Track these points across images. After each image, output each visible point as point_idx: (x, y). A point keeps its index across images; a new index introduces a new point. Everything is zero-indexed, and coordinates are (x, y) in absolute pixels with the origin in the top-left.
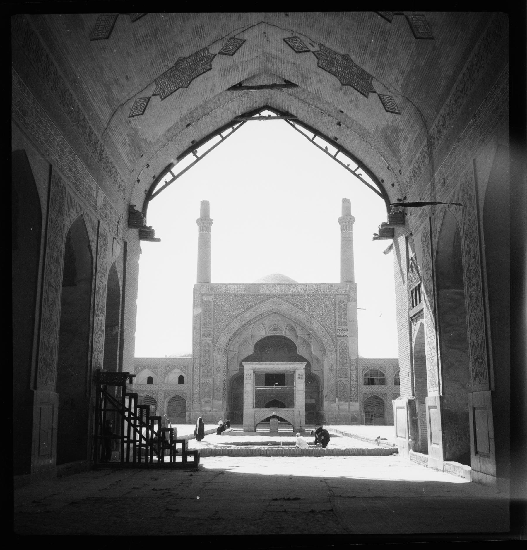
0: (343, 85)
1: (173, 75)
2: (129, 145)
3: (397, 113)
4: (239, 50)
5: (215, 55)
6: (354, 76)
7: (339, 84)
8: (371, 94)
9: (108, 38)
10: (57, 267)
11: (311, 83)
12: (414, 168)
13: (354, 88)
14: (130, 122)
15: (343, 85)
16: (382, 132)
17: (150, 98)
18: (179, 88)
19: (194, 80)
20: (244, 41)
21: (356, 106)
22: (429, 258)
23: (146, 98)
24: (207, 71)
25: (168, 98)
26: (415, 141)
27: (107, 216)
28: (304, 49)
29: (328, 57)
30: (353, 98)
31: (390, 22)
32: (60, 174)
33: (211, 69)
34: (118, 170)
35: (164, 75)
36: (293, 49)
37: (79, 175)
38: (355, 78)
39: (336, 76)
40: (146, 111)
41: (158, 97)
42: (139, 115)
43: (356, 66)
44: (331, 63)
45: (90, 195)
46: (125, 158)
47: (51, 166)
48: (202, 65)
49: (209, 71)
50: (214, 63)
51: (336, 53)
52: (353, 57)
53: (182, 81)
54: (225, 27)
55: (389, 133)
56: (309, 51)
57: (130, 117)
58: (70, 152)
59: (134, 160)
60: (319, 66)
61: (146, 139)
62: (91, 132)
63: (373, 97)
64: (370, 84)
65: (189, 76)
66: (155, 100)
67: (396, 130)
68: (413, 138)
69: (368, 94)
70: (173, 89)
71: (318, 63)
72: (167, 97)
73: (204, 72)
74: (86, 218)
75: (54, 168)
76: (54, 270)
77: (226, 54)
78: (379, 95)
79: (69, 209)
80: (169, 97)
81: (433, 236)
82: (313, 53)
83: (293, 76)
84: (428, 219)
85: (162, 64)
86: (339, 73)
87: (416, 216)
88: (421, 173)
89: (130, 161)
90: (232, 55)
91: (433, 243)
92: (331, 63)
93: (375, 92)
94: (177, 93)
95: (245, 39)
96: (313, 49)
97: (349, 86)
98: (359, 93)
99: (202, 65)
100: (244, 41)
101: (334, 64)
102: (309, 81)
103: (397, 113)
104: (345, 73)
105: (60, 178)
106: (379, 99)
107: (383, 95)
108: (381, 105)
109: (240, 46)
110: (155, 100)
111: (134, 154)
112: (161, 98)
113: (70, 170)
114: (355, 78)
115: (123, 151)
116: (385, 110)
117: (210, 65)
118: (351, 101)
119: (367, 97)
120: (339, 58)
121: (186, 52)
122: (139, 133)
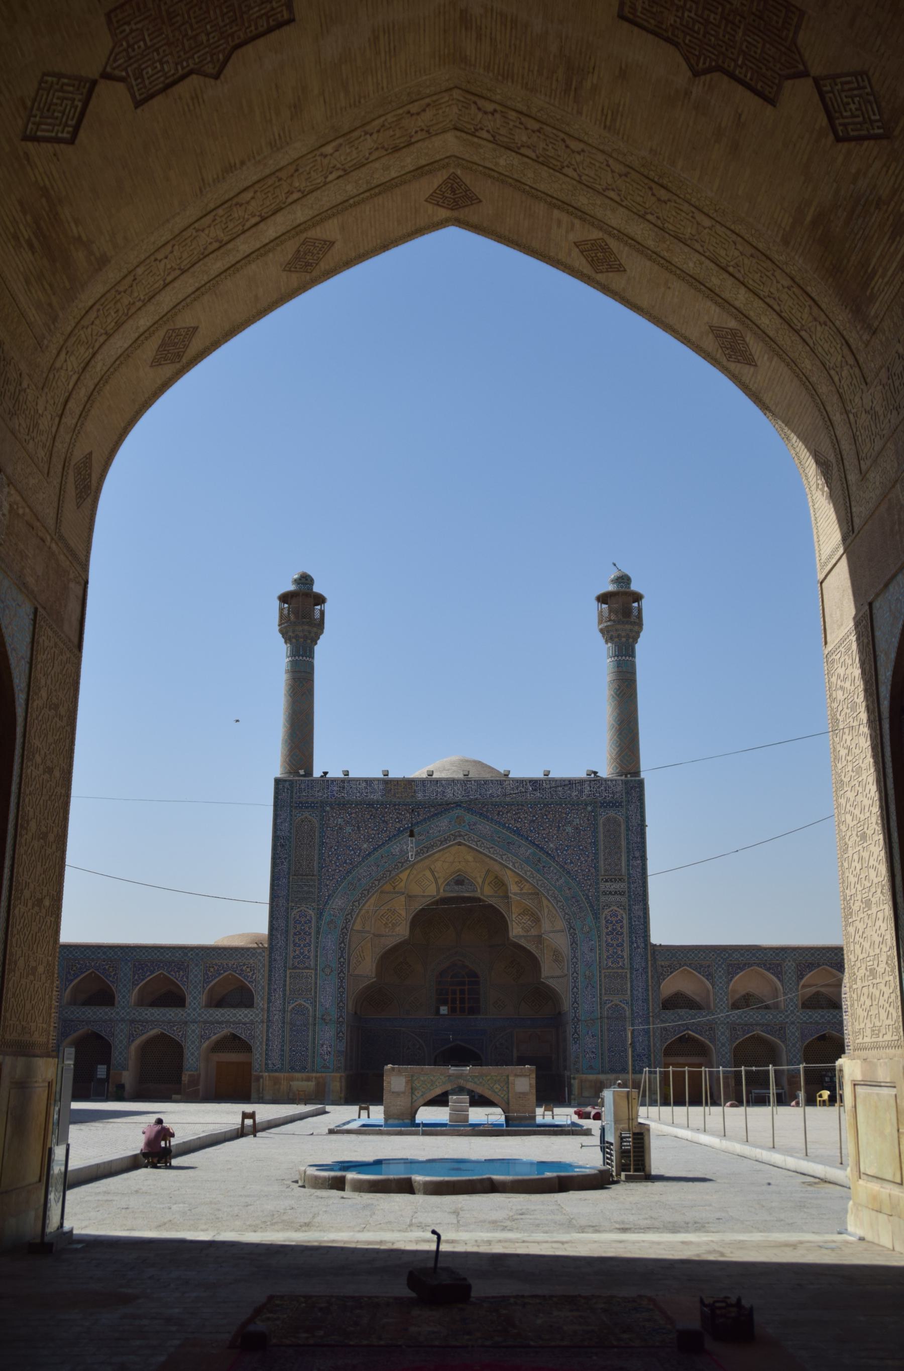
0: (696, 74)
2: (31, 246)
8: (788, 84)
13: (732, 76)
15: (696, 74)
18: (191, 72)
24: (280, 25)
25: (154, 102)
33: (291, 21)
39: (676, 45)
40: (82, 134)
41: (121, 86)
49: (287, 28)
57: (26, 138)
59: (50, 305)
60: (621, 17)
63: (798, 97)
66: (112, 99)
72: (152, 96)
73: (270, 30)
78: (816, 81)
80: (159, 98)
93: (805, 74)
98: (749, 94)
103: (876, 137)
106: (817, 95)
108: (823, 120)
110: (112, 99)
111: (51, 285)
112: (133, 96)
116: (831, 137)
119: (771, 101)
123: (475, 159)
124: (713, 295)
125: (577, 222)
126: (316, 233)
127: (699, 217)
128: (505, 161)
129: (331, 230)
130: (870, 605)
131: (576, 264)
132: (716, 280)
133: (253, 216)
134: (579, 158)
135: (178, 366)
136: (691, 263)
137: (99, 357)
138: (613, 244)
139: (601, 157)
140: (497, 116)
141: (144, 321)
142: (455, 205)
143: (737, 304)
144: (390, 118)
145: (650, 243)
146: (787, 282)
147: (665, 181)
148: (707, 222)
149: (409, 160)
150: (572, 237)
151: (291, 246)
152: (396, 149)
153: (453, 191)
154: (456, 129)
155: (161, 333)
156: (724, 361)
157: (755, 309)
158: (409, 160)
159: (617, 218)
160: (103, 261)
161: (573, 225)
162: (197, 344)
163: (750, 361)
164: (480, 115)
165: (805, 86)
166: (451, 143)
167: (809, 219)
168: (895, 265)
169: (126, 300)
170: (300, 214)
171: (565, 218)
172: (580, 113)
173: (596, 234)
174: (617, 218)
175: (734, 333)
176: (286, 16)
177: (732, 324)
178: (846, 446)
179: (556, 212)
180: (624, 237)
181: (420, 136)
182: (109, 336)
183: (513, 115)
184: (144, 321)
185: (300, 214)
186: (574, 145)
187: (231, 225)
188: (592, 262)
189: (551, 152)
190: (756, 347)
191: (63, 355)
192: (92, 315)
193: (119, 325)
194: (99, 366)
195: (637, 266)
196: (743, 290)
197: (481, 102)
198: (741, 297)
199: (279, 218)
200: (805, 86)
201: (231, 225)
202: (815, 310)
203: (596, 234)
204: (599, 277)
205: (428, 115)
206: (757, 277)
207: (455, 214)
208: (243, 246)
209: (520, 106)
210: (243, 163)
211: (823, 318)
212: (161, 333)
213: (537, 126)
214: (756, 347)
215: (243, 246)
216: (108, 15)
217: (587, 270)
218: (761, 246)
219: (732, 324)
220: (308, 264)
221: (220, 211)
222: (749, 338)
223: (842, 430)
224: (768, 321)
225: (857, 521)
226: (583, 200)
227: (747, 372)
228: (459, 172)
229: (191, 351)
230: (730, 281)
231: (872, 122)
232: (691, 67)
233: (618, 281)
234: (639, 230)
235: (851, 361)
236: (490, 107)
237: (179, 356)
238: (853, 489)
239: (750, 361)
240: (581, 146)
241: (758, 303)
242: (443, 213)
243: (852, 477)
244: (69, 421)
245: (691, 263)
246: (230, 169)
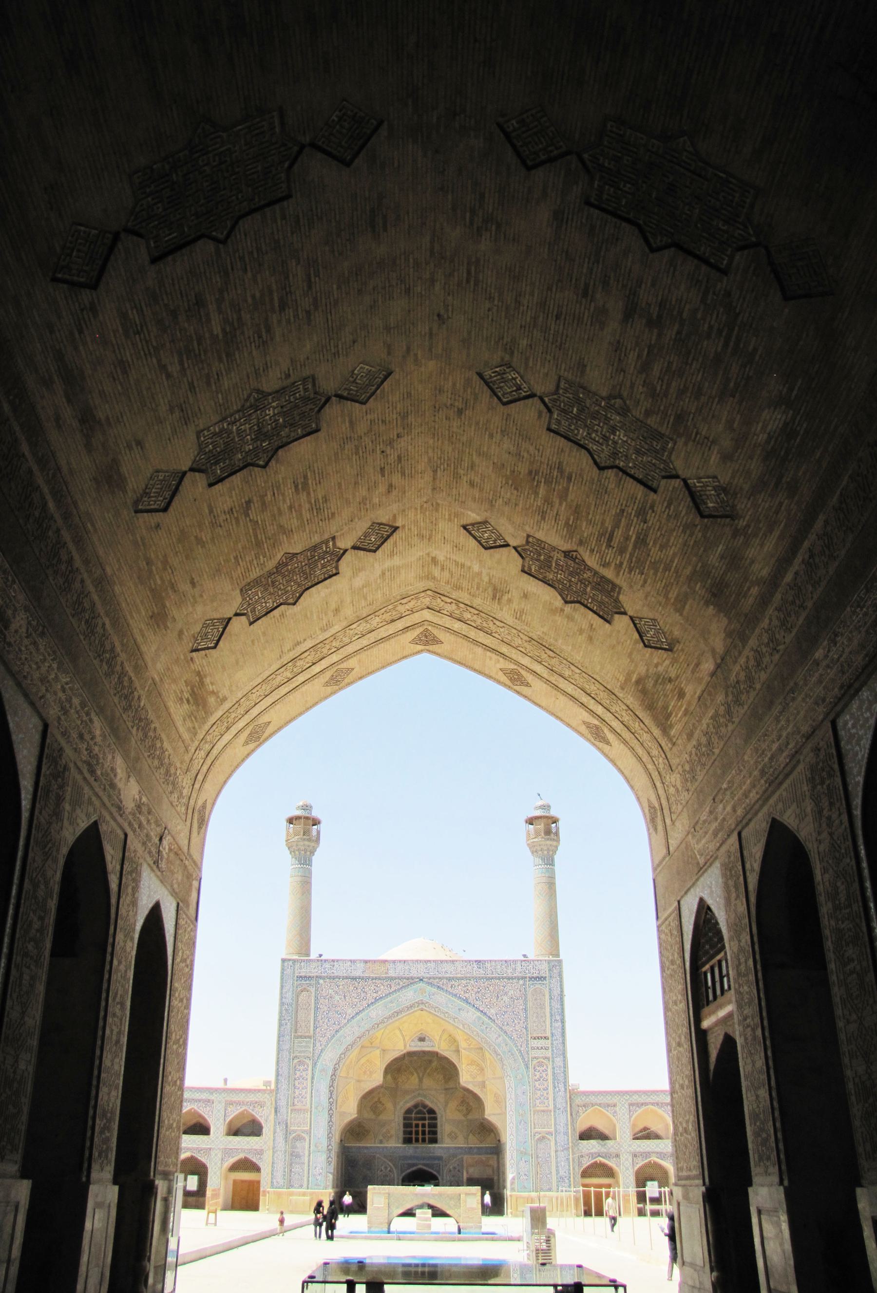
0: (566, 602)
1: (272, 582)
2: (188, 701)
3: (665, 649)
4: (385, 544)
5: (345, 551)
6: (586, 586)
7: (558, 602)
8: (617, 616)
9: (165, 510)
10: (41, 919)
11: (510, 601)
12: (699, 744)
14: (192, 659)
15: (566, 602)
16: (638, 682)
17: (230, 619)
18: (281, 604)
19: (307, 592)
20: (397, 528)
21: (590, 638)
22: (742, 908)
23: (223, 619)
24: (330, 577)
25: (260, 621)
26: (699, 698)
27: (140, 826)
28: (499, 543)
29: (540, 556)
30: (585, 625)
31: (655, 491)
32: (63, 742)
34: (166, 745)
35: (257, 582)
36: (479, 542)
37: (96, 749)
38: (589, 589)
40: (221, 643)
41: (243, 618)
42: (208, 648)
43: (590, 569)
44: (546, 565)
45: (113, 786)
46: (179, 723)
47: (46, 726)
48: (323, 566)
49: (334, 578)
50: (343, 564)
51: (554, 549)
52: (586, 556)
53: (286, 592)
54: (365, 504)
55: (650, 684)
56: (507, 545)
57: (193, 651)
58: (83, 705)
59: (194, 728)
60: (523, 571)
61: (218, 692)
62: (123, 673)
63: (622, 623)
64: (617, 601)
65: (299, 585)
66: (238, 625)
67: (663, 680)
68: (695, 693)
69: (612, 616)
70: (270, 605)
71: (523, 566)
72: (258, 619)
73: (325, 579)
74: (103, 828)
75: (53, 730)
76: (36, 925)
77: (364, 550)
78: (631, 618)
79: (74, 810)
81: (748, 866)
82: (515, 548)
83: (478, 588)
85: (255, 562)
86: (559, 581)
87: (706, 833)
88: (713, 753)
89: (189, 730)
90: (375, 551)
91: (749, 880)
92: (546, 565)
93: (625, 613)
94: (276, 613)
95: (397, 525)
96: (513, 543)
97: (577, 605)
98: (595, 616)
99: (323, 566)
100: (397, 528)
101: (550, 567)
102: (505, 597)
103: (665, 649)
104: (570, 581)
105: (61, 750)
106: (632, 625)
107: (641, 619)
108: (636, 635)
109: (388, 537)
110: (238, 625)
111: (196, 718)
112: (249, 620)
113: (81, 737)
114: (589, 589)
115: (178, 712)
116: (642, 644)
117: (337, 568)
118: (581, 631)
120: (561, 556)
121: (297, 544)
122: (208, 680)
123: (440, 623)
125: (501, 659)
126: (344, 665)
127: (573, 667)
128: (457, 626)
129: (352, 663)
130: (679, 902)
131: (502, 680)
132: (585, 699)
133: (308, 663)
134: (502, 630)
135: (258, 743)
136: (570, 689)
138: (523, 672)
139: (515, 631)
140: (453, 605)
141: (241, 724)
142: (427, 643)
144: (390, 607)
145: (545, 675)
147: (552, 648)
148: (578, 671)
149: (400, 625)
150: (499, 666)
151: (328, 675)
152: (393, 621)
153: (426, 637)
154: (428, 608)
155: (251, 728)
156: (593, 740)
157: (608, 717)
158: (400, 625)
159: (525, 661)
161: (499, 661)
164: (443, 603)
165: (625, 619)
166: (427, 615)
167: (634, 680)
168: (681, 713)
169: (233, 715)
170: (335, 658)
171: (494, 656)
172: (501, 610)
173: (512, 666)
174: (525, 661)
175: (597, 727)
176: (334, 571)
177: (596, 722)
179: (488, 654)
181: (407, 613)
182: (222, 735)
183: (462, 605)
184: (241, 724)
185: (335, 658)
186: (498, 623)
187: (295, 670)
189: (485, 625)
190: (610, 736)
193: (228, 728)
194: (215, 752)
195: (538, 686)
197: (443, 598)
198: (600, 710)
199: (323, 662)
200: (625, 619)
201: (295, 670)
202: (641, 724)
203: (512, 666)
205: (413, 603)
206: (608, 702)
207: (427, 647)
208: (301, 678)
209: (466, 602)
210: (305, 640)
211: (646, 730)
212: (251, 728)
213: (477, 612)
215: (301, 678)
216: (241, 590)
217: (508, 682)
218: (608, 687)
219: (596, 722)
220: (337, 681)
221: (290, 664)
223: (661, 792)
224: (615, 724)
225: (671, 849)
226: (504, 649)
227: (606, 748)
228: (430, 628)
229: (266, 735)
230: (593, 701)
231: (662, 642)
232: (563, 599)
234: (538, 668)
235: (663, 756)
236: (449, 600)
237: (259, 738)
238: (668, 828)
240: (502, 625)
241: (609, 714)
242: (419, 647)
243: (668, 821)
244: (197, 786)
245: (570, 689)
246: (298, 643)
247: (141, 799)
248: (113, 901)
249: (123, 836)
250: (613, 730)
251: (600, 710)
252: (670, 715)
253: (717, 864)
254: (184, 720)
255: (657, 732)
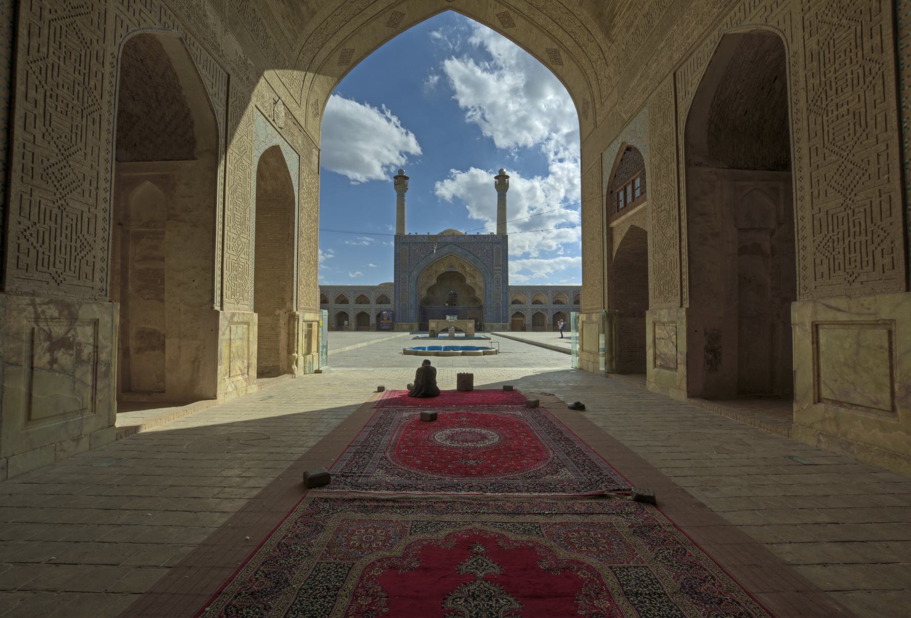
84: (671, 76)
124: (549, 34)
137: (316, 58)
138: (511, 14)
141: (333, 44)
143: (558, 37)
146: (579, 24)
160: (313, 13)
162: (355, 57)
163: (561, 64)
173: (505, 9)
175: (556, 51)
178: (596, 94)
180: (516, 10)
184: (333, 44)
188: (502, 24)
191: (301, 55)
192: (312, 38)
193: (323, 45)
195: (520, 23)
196: (561, 30)
198: (560, 34)
203: (505, 9)
204: (505, 30)
214: (564, 56)
217: (501, 27)
218: (570, 8)
219: (555, 47)
222: (562, 53)
224: (569, 44)
227: (559, 68)
233: (512, 31)
239: (561, 64)
241: (567, 36)
243: (597, 106)
247: (246, 60)
248: (221, 120)
249: (225, 75)
250: (567, 51)
251: (560, 34)
252: (614, 16)
253: (645, 110)
254: (283, 18)
255: (600, 37)
